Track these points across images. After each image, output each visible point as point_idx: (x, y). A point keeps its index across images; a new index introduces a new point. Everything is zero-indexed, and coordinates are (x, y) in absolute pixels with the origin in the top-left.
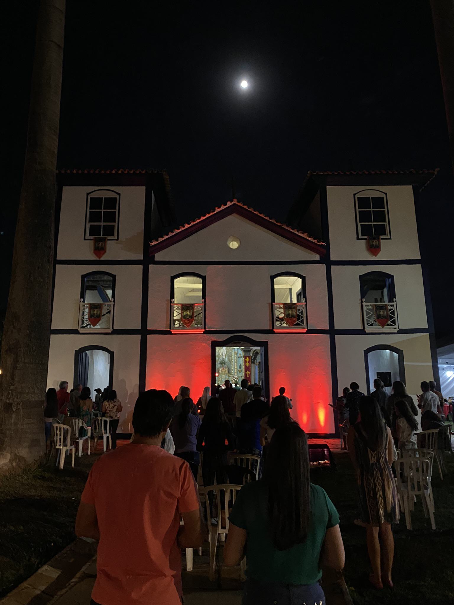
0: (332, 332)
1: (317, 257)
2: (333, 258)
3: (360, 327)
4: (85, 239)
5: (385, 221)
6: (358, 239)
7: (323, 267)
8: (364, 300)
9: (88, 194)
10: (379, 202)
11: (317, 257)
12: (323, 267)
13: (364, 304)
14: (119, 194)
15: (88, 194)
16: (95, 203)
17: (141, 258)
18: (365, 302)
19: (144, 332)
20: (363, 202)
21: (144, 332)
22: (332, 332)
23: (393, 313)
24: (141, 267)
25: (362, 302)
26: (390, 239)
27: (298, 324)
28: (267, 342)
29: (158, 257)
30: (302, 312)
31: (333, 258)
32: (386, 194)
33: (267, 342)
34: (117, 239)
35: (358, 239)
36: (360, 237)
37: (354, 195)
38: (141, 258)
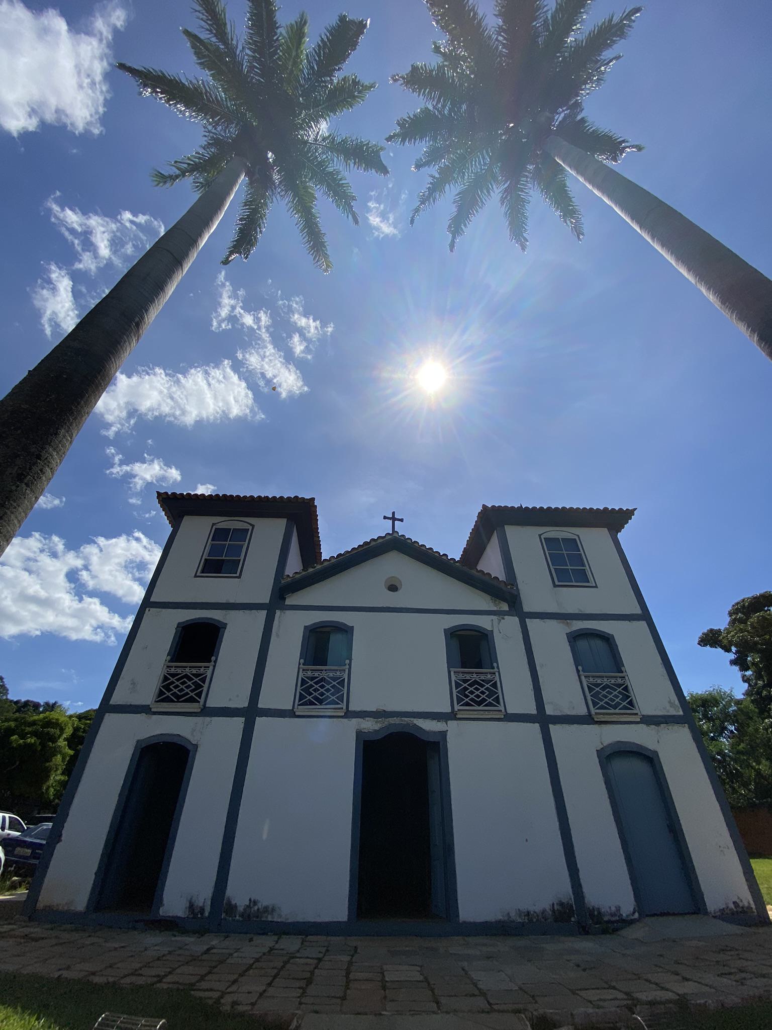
0: (543, 720)
2: (526, 609)
3: (583, 711)
4: (196, 576)
5: (583, 565)
6: (555, 586)
7: (516, 619)
8: (580, 668)
9: (214, 524)
10: (573, 544)
11: (505, 607)
13: (581, 673)
14: (253, 526)
15: (214, 524)
16: (220, 534)
18: (583, 671)
19: (251, 713)
20: (551, 543)
22: (543, 720)
23: (626, 689)
24: (264, 613)
25: (578, 671)
26: (596, 587)
27: (490, 704)
31: (526, 609)
34: (239, 577)
35: (555, 586)
36: (557, 583)
37: (540, 536)
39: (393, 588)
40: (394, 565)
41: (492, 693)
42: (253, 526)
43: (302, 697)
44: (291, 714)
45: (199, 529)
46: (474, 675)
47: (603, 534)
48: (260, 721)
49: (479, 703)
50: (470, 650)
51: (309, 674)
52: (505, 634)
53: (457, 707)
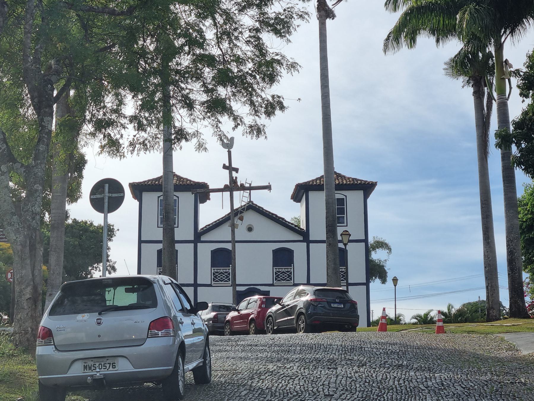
1: (302, 239)
2: (311, 238)
7: (306, 243)
9: (159, 197)
10: (341, 202)
11: (301, 238)
12: (306, 243)
14: (178, 197)
15: (159, 197)
17: (192, 238)
19: (196, 285)
21: (196, 285)
28: (269, 291)
29: (203, 238)
30: (291, 273)
31: (311, 238)
32: (346, 196)
33: (269, 291)
38: (192, 238)
39: (250, 229)
40: (250, 218)
41: (289, 276)
42: (178, 197)
43: (214, 280)
44: (210, 285)
45: (152, 199)
46: (283, 269)
47: (360, 194)
48: (199, 288)
49: (283, 280)
50: (283, 258)
51: (216, 271)
52: (299, 250)
53: (275, 282)
